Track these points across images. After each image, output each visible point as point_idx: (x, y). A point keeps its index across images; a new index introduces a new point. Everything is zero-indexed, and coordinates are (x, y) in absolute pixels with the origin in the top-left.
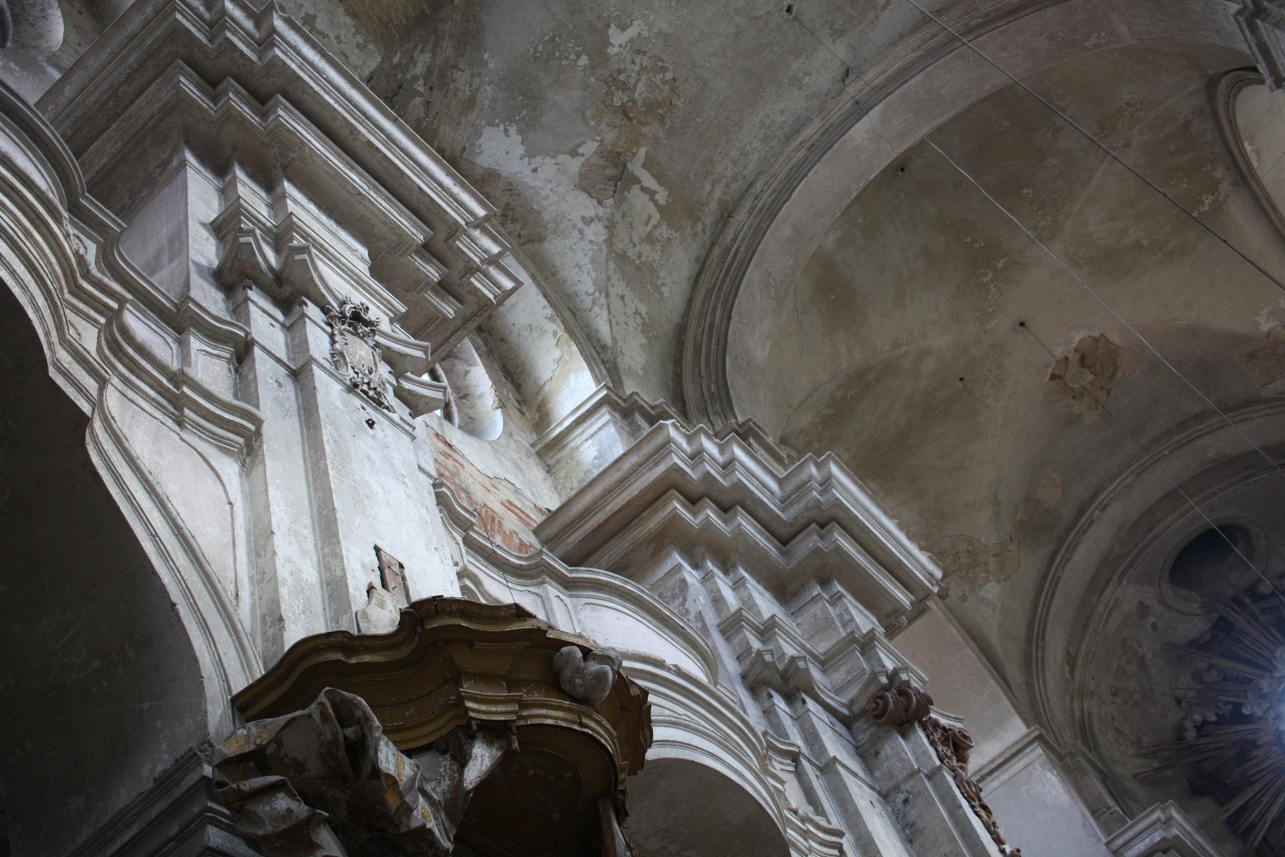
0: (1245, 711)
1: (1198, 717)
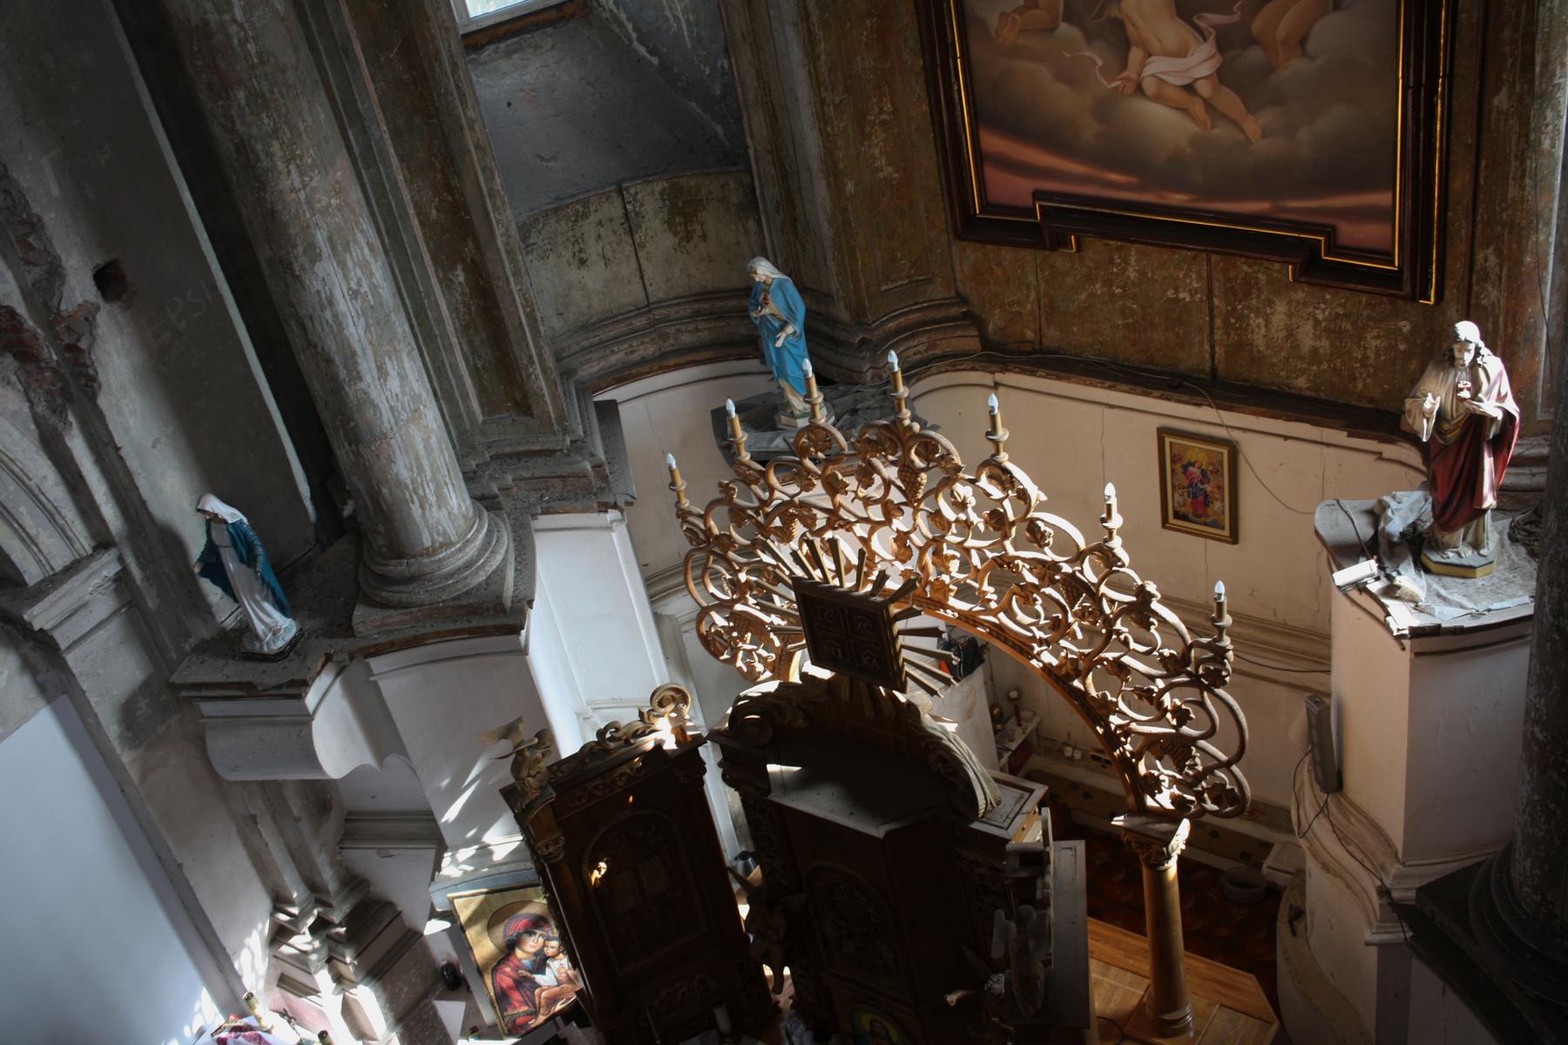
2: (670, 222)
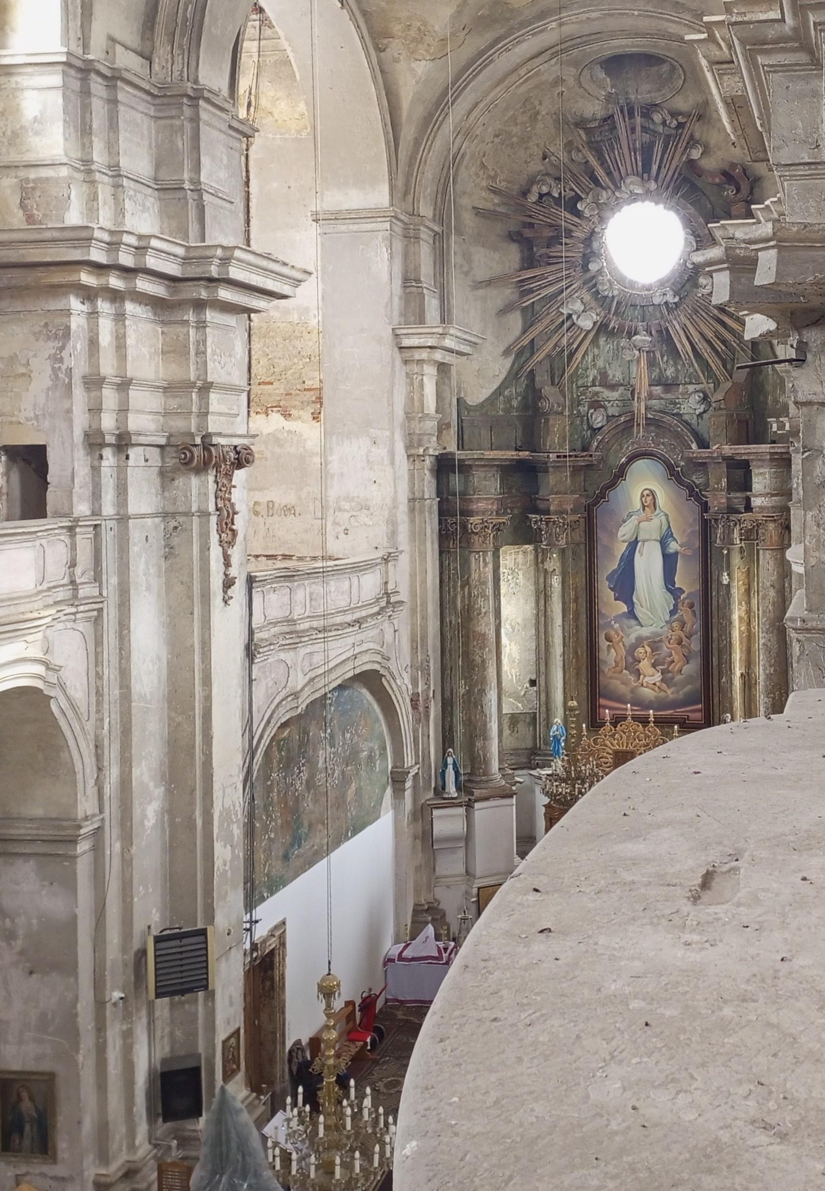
0: (579, 206)
1: (545, 189)
2: (510, 726)
